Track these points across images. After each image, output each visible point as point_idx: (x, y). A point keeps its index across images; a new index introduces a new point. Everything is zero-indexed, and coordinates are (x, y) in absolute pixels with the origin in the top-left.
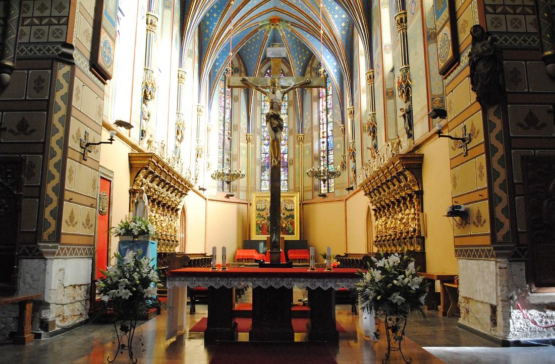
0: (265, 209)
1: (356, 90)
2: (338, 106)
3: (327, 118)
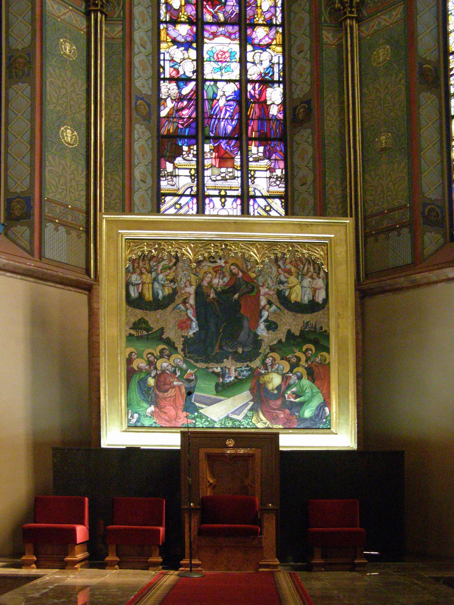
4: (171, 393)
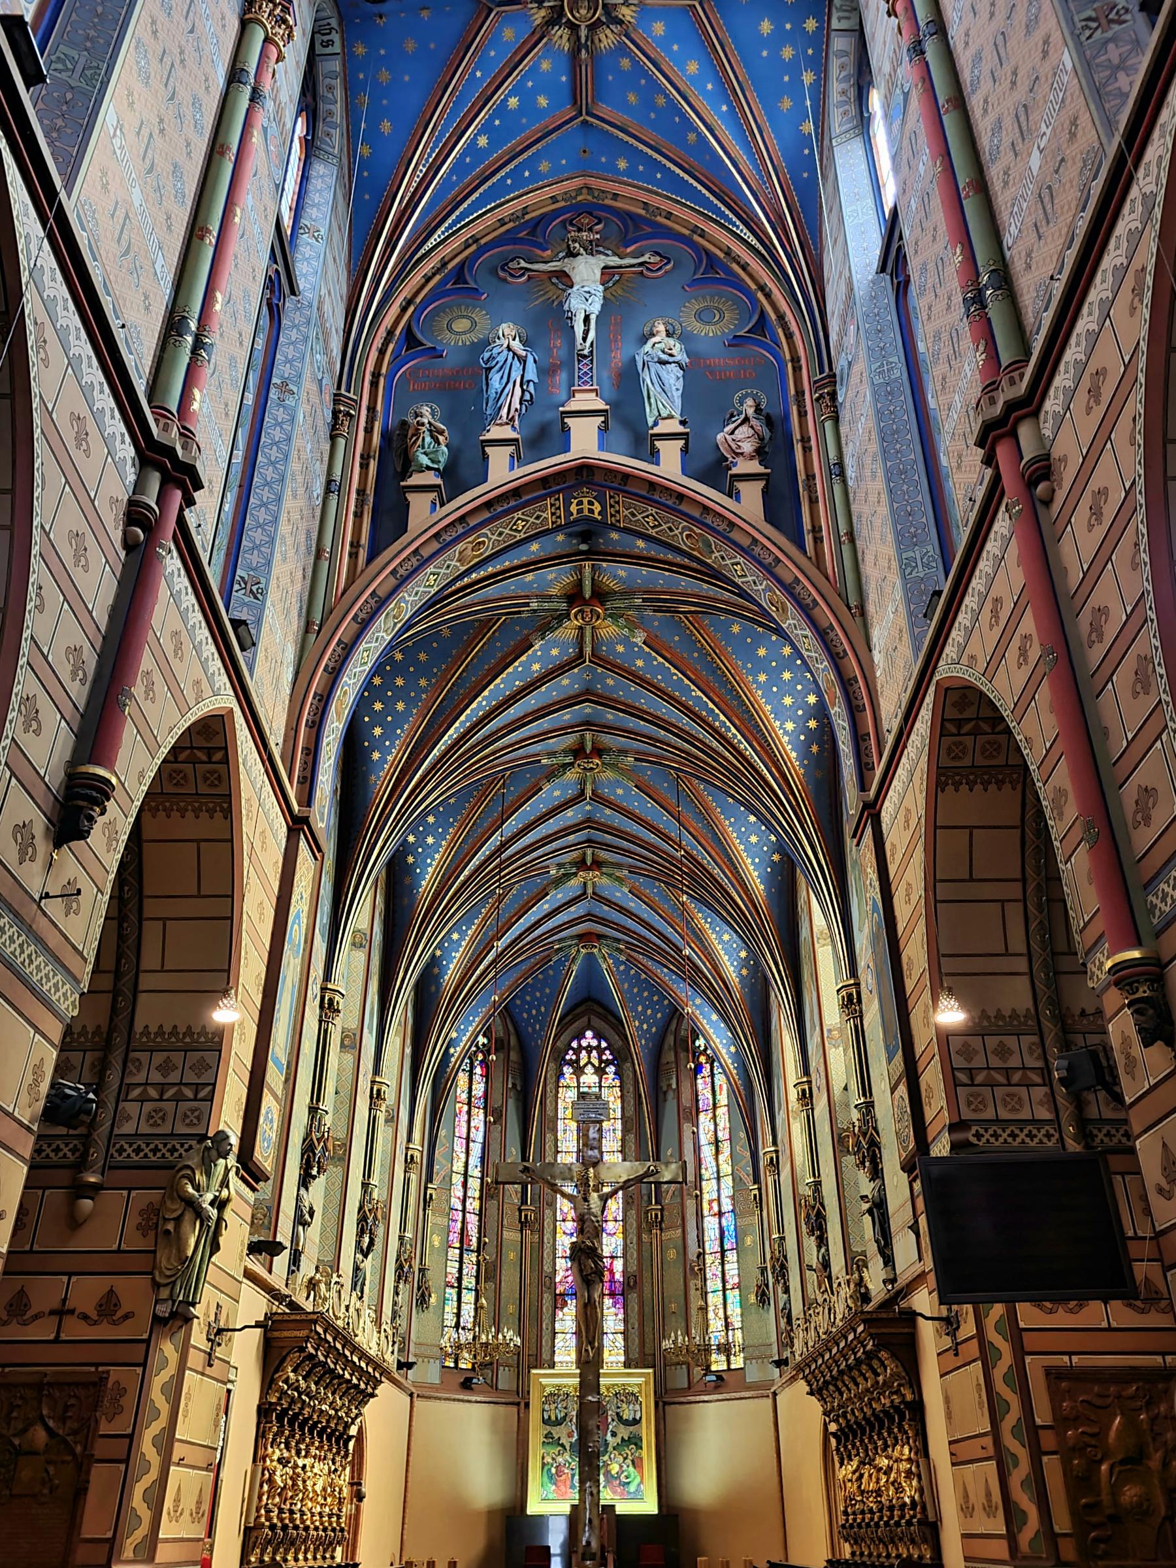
0: (564, 1418)
1: (780, 1109)
2: (743, 1135)
3: (718, 1166)
4: (564, 1477)
